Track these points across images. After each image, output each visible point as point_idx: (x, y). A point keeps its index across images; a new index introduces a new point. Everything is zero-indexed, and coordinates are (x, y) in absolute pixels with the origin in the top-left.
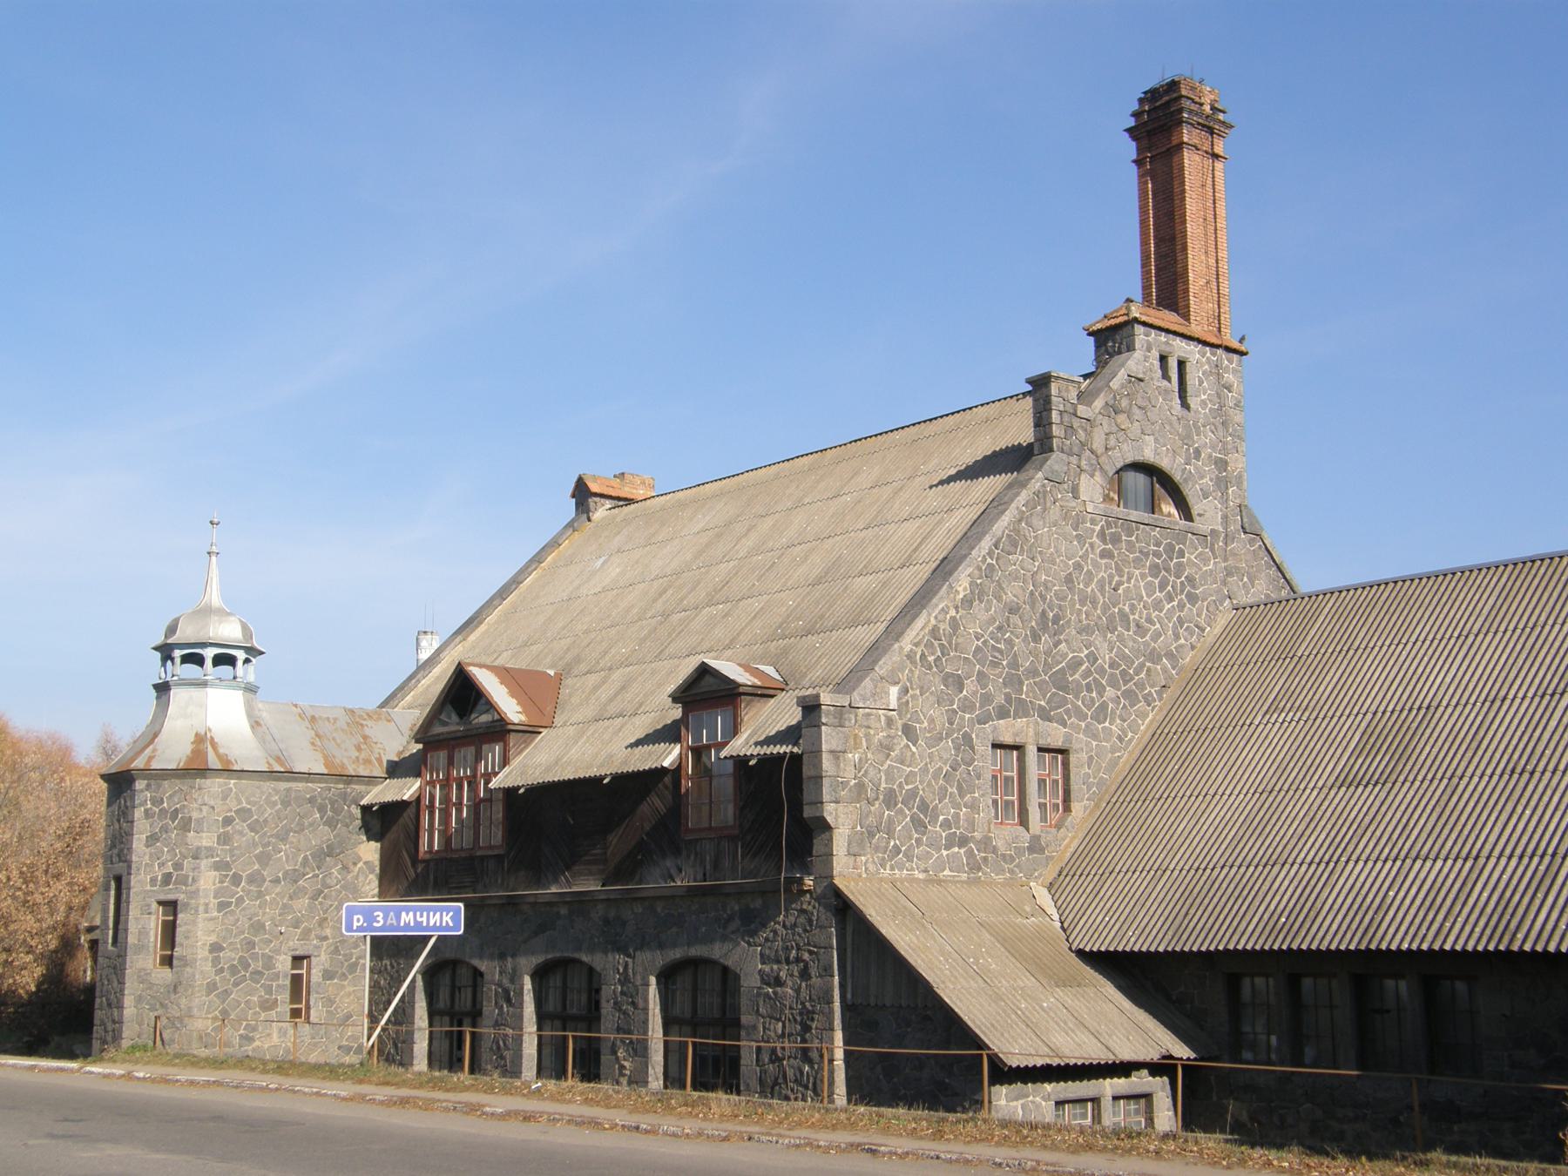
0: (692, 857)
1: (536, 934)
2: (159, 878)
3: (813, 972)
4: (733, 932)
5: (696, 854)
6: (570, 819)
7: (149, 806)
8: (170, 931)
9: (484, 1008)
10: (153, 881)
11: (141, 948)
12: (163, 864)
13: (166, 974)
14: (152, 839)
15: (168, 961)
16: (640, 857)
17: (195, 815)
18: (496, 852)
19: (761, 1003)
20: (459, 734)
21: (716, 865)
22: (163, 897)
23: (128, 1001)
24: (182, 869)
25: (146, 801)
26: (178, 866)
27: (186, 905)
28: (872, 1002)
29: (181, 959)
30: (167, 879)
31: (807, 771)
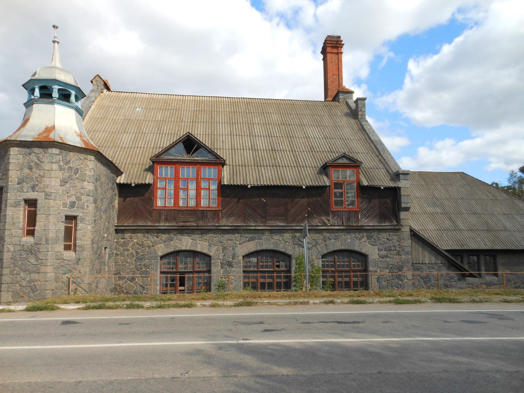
0: (336, 217)
1: (249, 241)
2: (68, 204)
3: (402, 253)
4: (364, 242)
5: (338, 216)
6: (263, 200)
7: (62, 164)
8: (69, 234)
9: (212, 270)
10: (65, 205)
11: (56, 241)
12: (70, 196)
13: (70, 255)
14: (64, 182)
15: (67, 248)
16: (306, 215)
17: (88, 173)
18: (214, 209)
19: (379, 263)
20: (187, 161)
21: (348, 219)
22: (70, 214)
23: (49, 269)
24: (81, 200)
25: (60, 160)
26: (79, 199)
27: (83, 220)
28: (421, 262)
29: (80, 246)
30: (73, 205)
31: (403, 192)
